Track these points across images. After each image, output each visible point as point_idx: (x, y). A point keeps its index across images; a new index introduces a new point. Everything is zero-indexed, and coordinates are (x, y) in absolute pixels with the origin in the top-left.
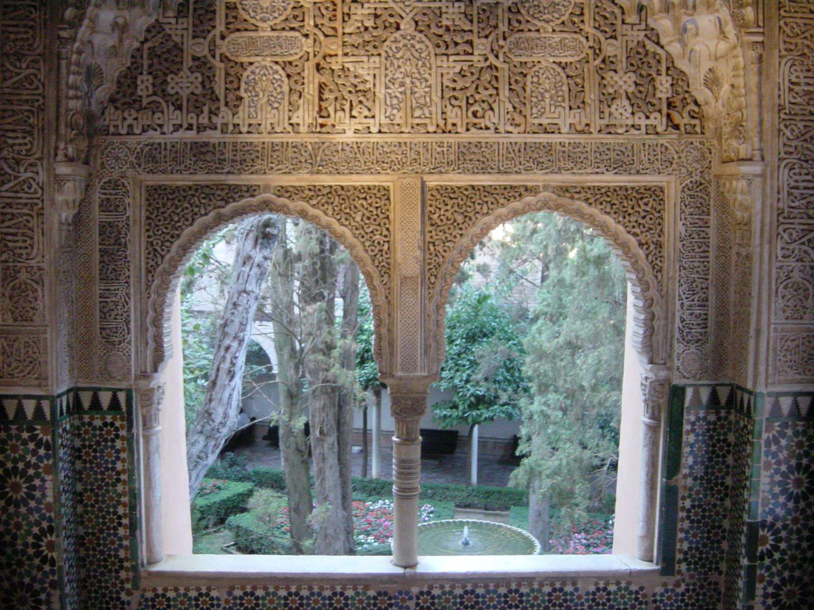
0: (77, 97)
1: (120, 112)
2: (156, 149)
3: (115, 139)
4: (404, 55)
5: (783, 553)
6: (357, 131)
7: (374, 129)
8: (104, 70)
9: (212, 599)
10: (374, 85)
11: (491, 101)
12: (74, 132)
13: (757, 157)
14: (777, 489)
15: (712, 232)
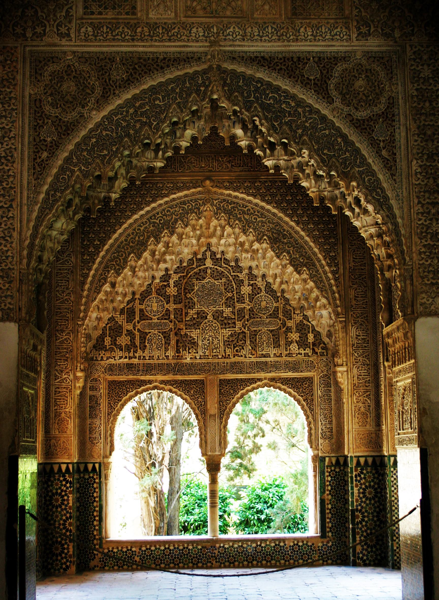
3: (96, 362)
5: (367, 522)
7: (198, 357)
9: (133, 552)
13: (345, 364)
14: (361, 495)
15: (332, 394)
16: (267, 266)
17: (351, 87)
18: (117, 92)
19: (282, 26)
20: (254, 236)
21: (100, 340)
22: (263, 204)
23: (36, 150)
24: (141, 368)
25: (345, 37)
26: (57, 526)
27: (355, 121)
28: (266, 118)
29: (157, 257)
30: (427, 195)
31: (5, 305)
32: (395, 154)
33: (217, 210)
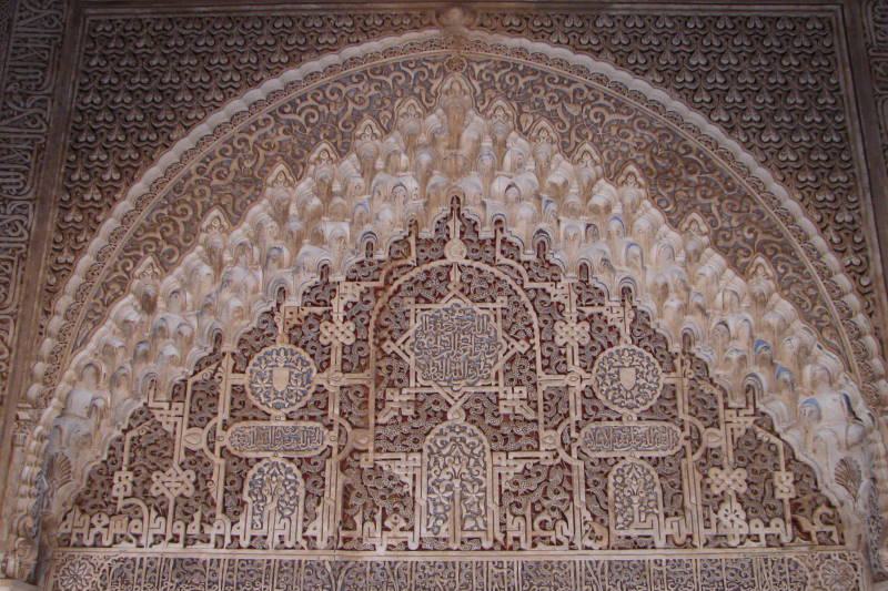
0: (30, 496)
1: (87, 517)
2: (128, 567)
4: (451, 451)
7: (413, 545)
8: (72, 463)
10: (414, 489)
11: (563, 507)
12: (21, 539)
20: (596, 164)
21: (99, 479)
22: (623, 76)
24: (222, 576)
29: (295, 225)
33: (483, 92)
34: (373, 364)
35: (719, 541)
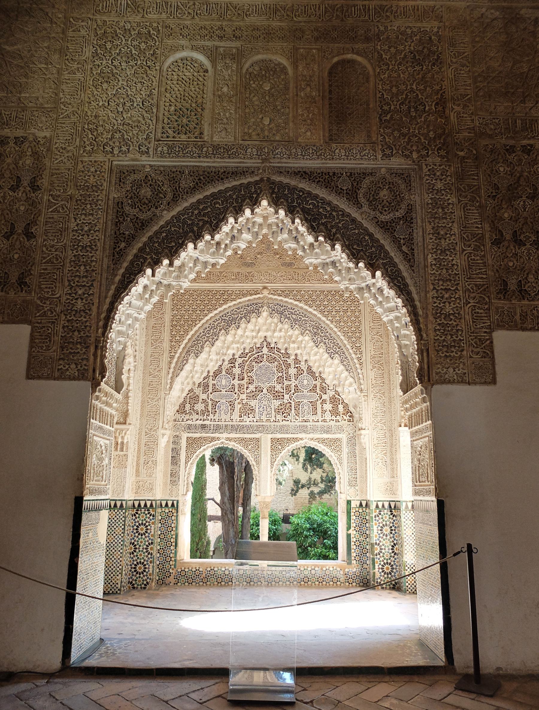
6: (250, 421)
7: (255, 421)
16: (309, 354)
17: (377, 196)
18: (185, 197)
19: (321, 148)
22: (306, 307)
23: (116, 241)
24: (212, 428)
25: (372, 157)
26: (141, 549)
27: (379, 223)
28: (306, 220)
29: (226, 345)
30: (441, 283)
31: (81, 367)
32: (413, 250)
34: (245, 378)
35: (324, 421)
